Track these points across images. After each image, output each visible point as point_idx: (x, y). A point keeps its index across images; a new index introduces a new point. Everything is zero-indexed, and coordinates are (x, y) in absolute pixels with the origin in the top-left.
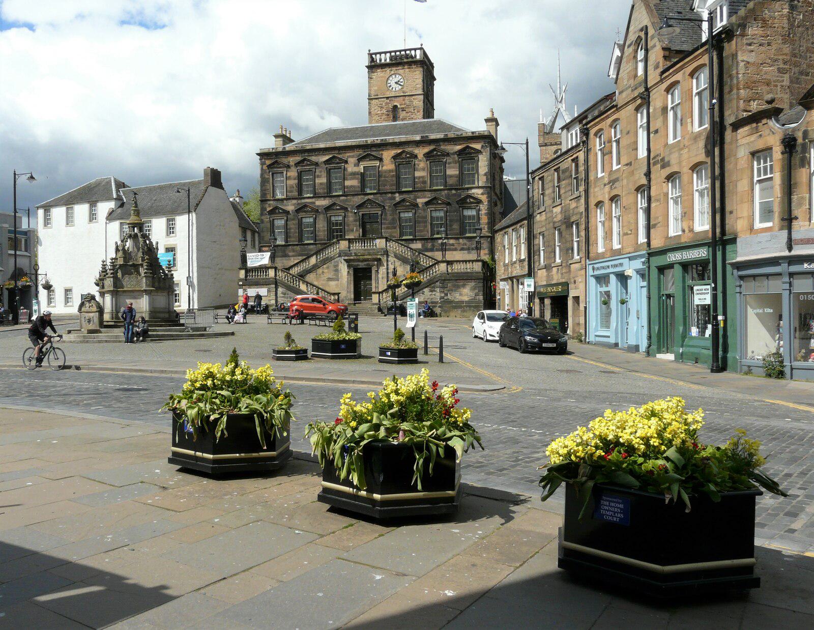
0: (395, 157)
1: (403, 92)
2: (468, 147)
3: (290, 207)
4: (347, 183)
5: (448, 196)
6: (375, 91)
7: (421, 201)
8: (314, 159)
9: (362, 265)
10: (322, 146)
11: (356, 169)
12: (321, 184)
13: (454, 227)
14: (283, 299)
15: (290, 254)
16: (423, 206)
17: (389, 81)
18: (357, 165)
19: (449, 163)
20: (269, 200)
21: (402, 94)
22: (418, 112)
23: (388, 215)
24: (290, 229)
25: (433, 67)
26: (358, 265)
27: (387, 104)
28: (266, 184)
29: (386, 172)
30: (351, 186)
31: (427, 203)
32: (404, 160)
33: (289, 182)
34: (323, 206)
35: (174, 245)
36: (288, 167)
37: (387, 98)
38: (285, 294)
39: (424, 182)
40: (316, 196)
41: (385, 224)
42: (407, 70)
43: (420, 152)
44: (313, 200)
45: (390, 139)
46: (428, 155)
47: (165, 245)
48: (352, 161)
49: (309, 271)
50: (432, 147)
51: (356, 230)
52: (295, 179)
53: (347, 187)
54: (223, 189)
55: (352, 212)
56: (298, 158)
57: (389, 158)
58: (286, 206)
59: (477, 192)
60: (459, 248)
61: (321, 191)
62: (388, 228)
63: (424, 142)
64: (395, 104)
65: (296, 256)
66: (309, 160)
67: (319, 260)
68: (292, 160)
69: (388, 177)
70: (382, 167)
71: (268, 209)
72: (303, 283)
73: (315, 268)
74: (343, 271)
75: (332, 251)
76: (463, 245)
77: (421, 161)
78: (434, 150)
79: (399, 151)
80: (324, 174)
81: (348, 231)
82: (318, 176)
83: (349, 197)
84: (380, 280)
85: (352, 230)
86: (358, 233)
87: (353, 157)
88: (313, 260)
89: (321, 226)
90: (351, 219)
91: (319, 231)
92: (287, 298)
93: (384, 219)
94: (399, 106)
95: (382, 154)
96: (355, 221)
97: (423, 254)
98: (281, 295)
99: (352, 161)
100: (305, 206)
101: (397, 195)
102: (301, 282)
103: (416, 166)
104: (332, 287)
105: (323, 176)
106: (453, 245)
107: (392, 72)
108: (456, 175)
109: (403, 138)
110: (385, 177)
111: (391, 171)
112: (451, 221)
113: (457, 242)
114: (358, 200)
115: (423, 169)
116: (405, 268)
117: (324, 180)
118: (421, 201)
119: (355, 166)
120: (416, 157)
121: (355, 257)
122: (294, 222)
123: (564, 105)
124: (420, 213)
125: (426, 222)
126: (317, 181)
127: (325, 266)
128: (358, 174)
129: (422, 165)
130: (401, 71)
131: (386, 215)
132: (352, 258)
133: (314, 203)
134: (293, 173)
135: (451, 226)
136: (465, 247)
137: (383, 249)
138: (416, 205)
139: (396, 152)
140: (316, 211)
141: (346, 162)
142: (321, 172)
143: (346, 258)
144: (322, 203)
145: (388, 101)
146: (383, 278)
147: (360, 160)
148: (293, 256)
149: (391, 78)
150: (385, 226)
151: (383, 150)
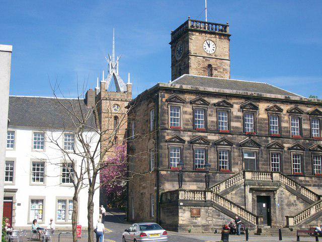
2: (317, 110)
3: (187, 139)
4: (234, 124)
5: (303, 143)
8: (206, 99)
9: (263, 194)
12: (212, 122)
13: (309, 168)
15: (187, 179)
19: (304, 120)
20: (167, 129)
22: (226, 73)
24: (186, 157)
30: (237, 128)
31: (289, 149)
32: (275, 113)
34: (213, 140)
35: (13, 158)
36: (183, 102)
37: (204, 57)
40: (206, 130)
41: (261, 161)
42: (218, 39)
43: (285, 108)
44: (205, 134)
46: (290, 112)
48: (236, 107)
50: (293, 106)
52: (190, 114)
56: (193, 97)
58: (182, 136)
60: (312, 185)
61: (212, 128)
62: (263, 164)
63: (287, 101)
65: (191, 181)
66: (204, 101)
68: (188, 97)
71: (167, 138)
73: (226, 192)
76: (315, 182)
77: (285, 115)
78: (295, 109)
80: (214, 114)
81: (234, 164)
82: (210, 115)
83: (234, 136)
87: (237, 103)
89: (212, 157)
90: (236, 154)
91: (210, 162)
95: (258, 105)
97: (305, 188)
99: (236, 107)
101: (269, 139)
102: (232, 205)
105: (214, 115)
106: (308, 182)
107: (207, 38)
109: (273, 96)
111: (264, 119)
114: (242, 139)
118: (286, 145)
120: (281, 110)
122: (189, 151)
123: (118, 72)
126: (209, 119)
127: (234, 192)
129: (286, 118)
130: (214, 39)
131: (262, 154)
132: (255, 187)
133: (207, 137)
134: (189, 109)
135: (306, 167)
138: (282, 148)
140: (207, 142)
141: (232, 106)
142: (212, 112)
143: (251, 187)
144: (212, 137)
148: (189, 181)
150: (262, 163)
151: (259, 102)
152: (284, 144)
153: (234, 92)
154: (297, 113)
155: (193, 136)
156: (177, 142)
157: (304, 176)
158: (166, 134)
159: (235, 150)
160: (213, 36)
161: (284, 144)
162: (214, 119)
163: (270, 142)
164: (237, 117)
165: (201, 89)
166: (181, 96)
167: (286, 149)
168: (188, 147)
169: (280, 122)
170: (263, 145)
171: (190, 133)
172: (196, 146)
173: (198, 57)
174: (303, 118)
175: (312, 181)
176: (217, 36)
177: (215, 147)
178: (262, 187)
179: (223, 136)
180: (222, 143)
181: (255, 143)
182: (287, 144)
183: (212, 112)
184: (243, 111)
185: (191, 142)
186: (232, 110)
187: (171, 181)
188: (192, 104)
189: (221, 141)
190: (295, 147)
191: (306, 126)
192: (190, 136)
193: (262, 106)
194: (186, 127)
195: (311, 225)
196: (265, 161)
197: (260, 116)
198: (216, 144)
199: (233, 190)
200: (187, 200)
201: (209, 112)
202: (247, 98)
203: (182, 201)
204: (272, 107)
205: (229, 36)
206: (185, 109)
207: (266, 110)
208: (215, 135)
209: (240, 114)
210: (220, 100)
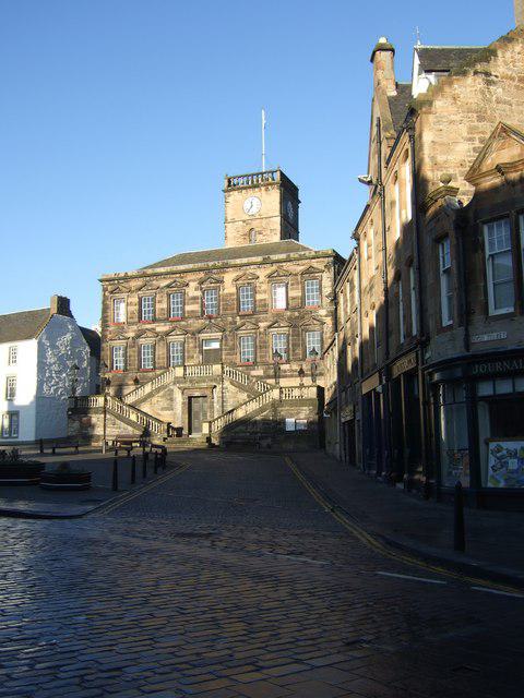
3: (131, 334)
4: (188, 308)
10: (162, 270)
25: (296, 189)
30: (192, 311)
33: (131, 308)
37: (244, 221)
40: (154, 320)
44: (152, 326)
45: (232, 262)
48: (193, 285)
49: (144, 400)
50: (274, 267)
54: (72, 317)
73: (150, 395)
75: (168, 379)
79: (241, 273)
85: (193, 357)
87: (194, 281)
88: (148, 389)
90: (191, 345)
99: (193, 285)
103: (258, 289)
104: (166, 416)
109: (245, 260)
111: (231, 294)
117: (165, 306)
126: (158, 306)
129: (264, 287)
130: (258, 194)
144: (161, 328)
151: (224, 272)
152: (260, 324)
153: (191, 266)
161: (260, 324)
164: (195, 298)
165: (150, 271)
167: (262, 330)
169: (255, 292)
176: (263, 188)
184: (201, 289)
186: (187, 290)
195: (236, 433)
196: (230, 349)
197: (226, 291)
202: (207, 270)
206: (130, 300)
209: (199, 293)
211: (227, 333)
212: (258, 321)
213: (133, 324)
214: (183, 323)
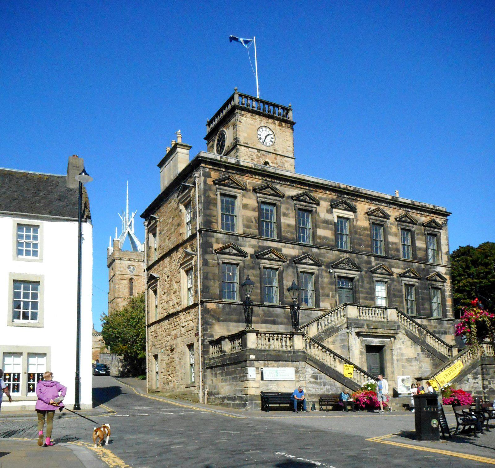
0: (369, 214)
1: (275, 150)
4: (321, 232)
6: (245, 138)
7: (396, 271)
9: (376, 342)
11: (329, 217)
12: (289, 226)
14: (314, 385)
16: (397, 277)
17: (259, 133)
18: (330, 212)
20: (216, 231)
21: (273, 152)
23: (365, 282)
26: (371, 342)
27: (258, 157)
28: (212, 207)
29: (360, 228)
30: (325, 238)
37: (259, 150)
38: (316, 378)
39: (398, 250)
40: (281, 239)
41: (362, 293)
42: (278, 127)
46: (399, 220)
47: (10, 274)
51: (333, 297)
52: (254, 210)
53: (320, 237)
55: (326, 271)
57: (363, 213)
58: (241, 246)
59: (442, 270)
61: (289, 235)
64: (267, 160)
66: (274, 189)
67: (320, 331)
68: (251, 181)
69: (362, 235)
70: (357, 221)
71: (216, 246)
72: (340, 362)
74: (354, 349)
78: (405, 216)
79: (373, 207)
80: (292, 213)
82: (285, 215)
83: (322, 251)
84: (395, 362)
85: (328, 296)
86: (334, 299)
87: (325, 200)
90: (326, 280)
92: (320, 384)
93: (362, 287)
94: (271, 164)
96: (331, 283)
98: (313, 380)
99: (324, 205)
100: (270, 250)
101: (373, 258)
102: (337, 360)
105: (291, 215)
107: (263, 124)
108: (423, 248)
110: (360, 235)
111: (365, 229)
112: (423, 299)
113: (429, 324)
114: (332, 255)
115: (396, 235)
116: (415, 349)
118: (396, 271)
119: (328, 212)
121: (367, 330)
124: (395, 286)
125: (401, 297)
126: (284, 220)
128: (331, 224)
130: (271, 126)
131: (363, 282)
133: (280, 250)
134: (252, 200)
135: (423, 305)
136: (436, 330)
137: (395, 322)
138: (391, 274)
139: (369, 207)
141: (318, 204)
142: (288, 209)
144: (290, 251)
145: (259, 154)
146: (397, 361)
147: (334, 205)
149: (261, 130)
151: (356, 200)
152: (393, 270)
154: (408, 223)
155: (259, 247)
156: (234, 255)
157: (421, 318)
158: (213, 240)
159: (324, 274)
160: (270, 121)
162: (292, 221)
163: (373, 264)
166: (237, 177)
167: (395, 276)
168: (251, 265)
170: (364, 267)
171: (253, 242)
172: (264, 263)
173: (250, 149)
174: (417, 231)
175: (431, 325)
176: (277, 122)
177: (293, 268)
178: (374, 330)
179: (305, 249)
180: (304, 261)
181: (354, 264)
182: (396, 268)
183: (288, 209)
185: (259, 255)
187: (224, 321)
188: (256, 193)
189: (305, 258)
190: (407, 274)
191: (420, 244)
192: (254, 246)
193: (362, 207)
194: (248, 231)
196: (367, 293)
198: (297, 261)
199: (329, 336)
200: (260, 351)
201: (283, 209)
203: (253, 351)
204: (375, 211)
205: (292, 123)
207: (367, 213)
208: (293, 248)
210: (300, 192)
211: (363, 273)
212: (391, 266)
213: (253, 237)
214: (315, 250)
